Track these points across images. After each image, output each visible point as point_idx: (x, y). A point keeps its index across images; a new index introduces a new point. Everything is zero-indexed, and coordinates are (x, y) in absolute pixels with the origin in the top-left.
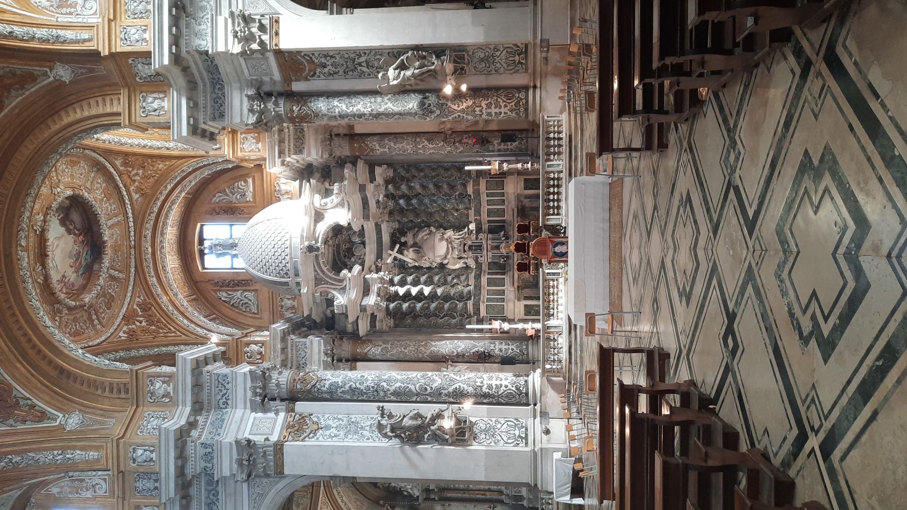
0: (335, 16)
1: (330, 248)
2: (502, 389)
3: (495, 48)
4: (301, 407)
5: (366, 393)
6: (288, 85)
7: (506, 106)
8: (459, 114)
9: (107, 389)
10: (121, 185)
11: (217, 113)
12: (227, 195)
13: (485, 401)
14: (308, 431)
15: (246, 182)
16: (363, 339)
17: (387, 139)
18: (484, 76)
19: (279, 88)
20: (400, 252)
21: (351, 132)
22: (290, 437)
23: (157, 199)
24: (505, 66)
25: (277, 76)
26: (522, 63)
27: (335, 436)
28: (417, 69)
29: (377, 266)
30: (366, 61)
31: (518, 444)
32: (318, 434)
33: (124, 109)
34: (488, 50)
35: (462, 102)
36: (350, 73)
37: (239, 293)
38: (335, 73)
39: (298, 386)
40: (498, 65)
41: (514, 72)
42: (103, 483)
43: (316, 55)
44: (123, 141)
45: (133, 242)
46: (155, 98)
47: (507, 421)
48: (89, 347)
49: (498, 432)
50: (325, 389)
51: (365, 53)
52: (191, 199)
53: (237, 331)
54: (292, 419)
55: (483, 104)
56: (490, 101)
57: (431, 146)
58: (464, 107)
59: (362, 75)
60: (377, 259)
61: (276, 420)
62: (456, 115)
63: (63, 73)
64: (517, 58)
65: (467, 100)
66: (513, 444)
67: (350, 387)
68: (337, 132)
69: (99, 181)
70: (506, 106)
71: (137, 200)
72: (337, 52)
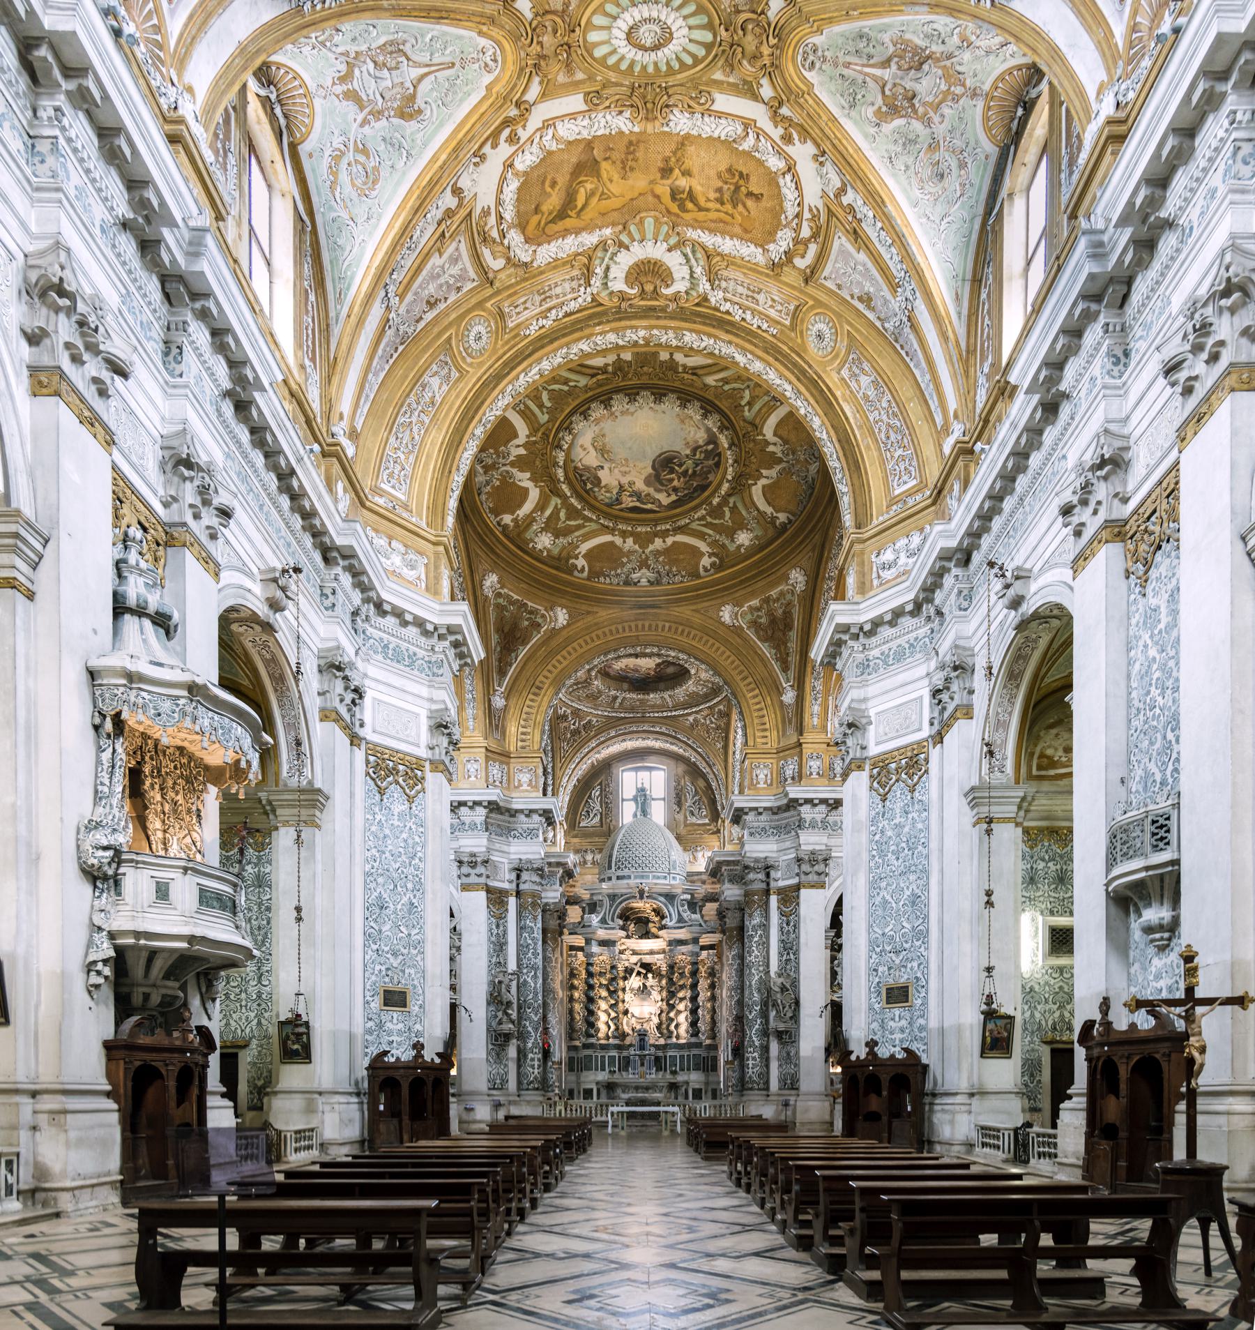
19: (773, 884)
25: (781, 884)
37: (598, 807)
59: (781, 955)
63: (789, 697)
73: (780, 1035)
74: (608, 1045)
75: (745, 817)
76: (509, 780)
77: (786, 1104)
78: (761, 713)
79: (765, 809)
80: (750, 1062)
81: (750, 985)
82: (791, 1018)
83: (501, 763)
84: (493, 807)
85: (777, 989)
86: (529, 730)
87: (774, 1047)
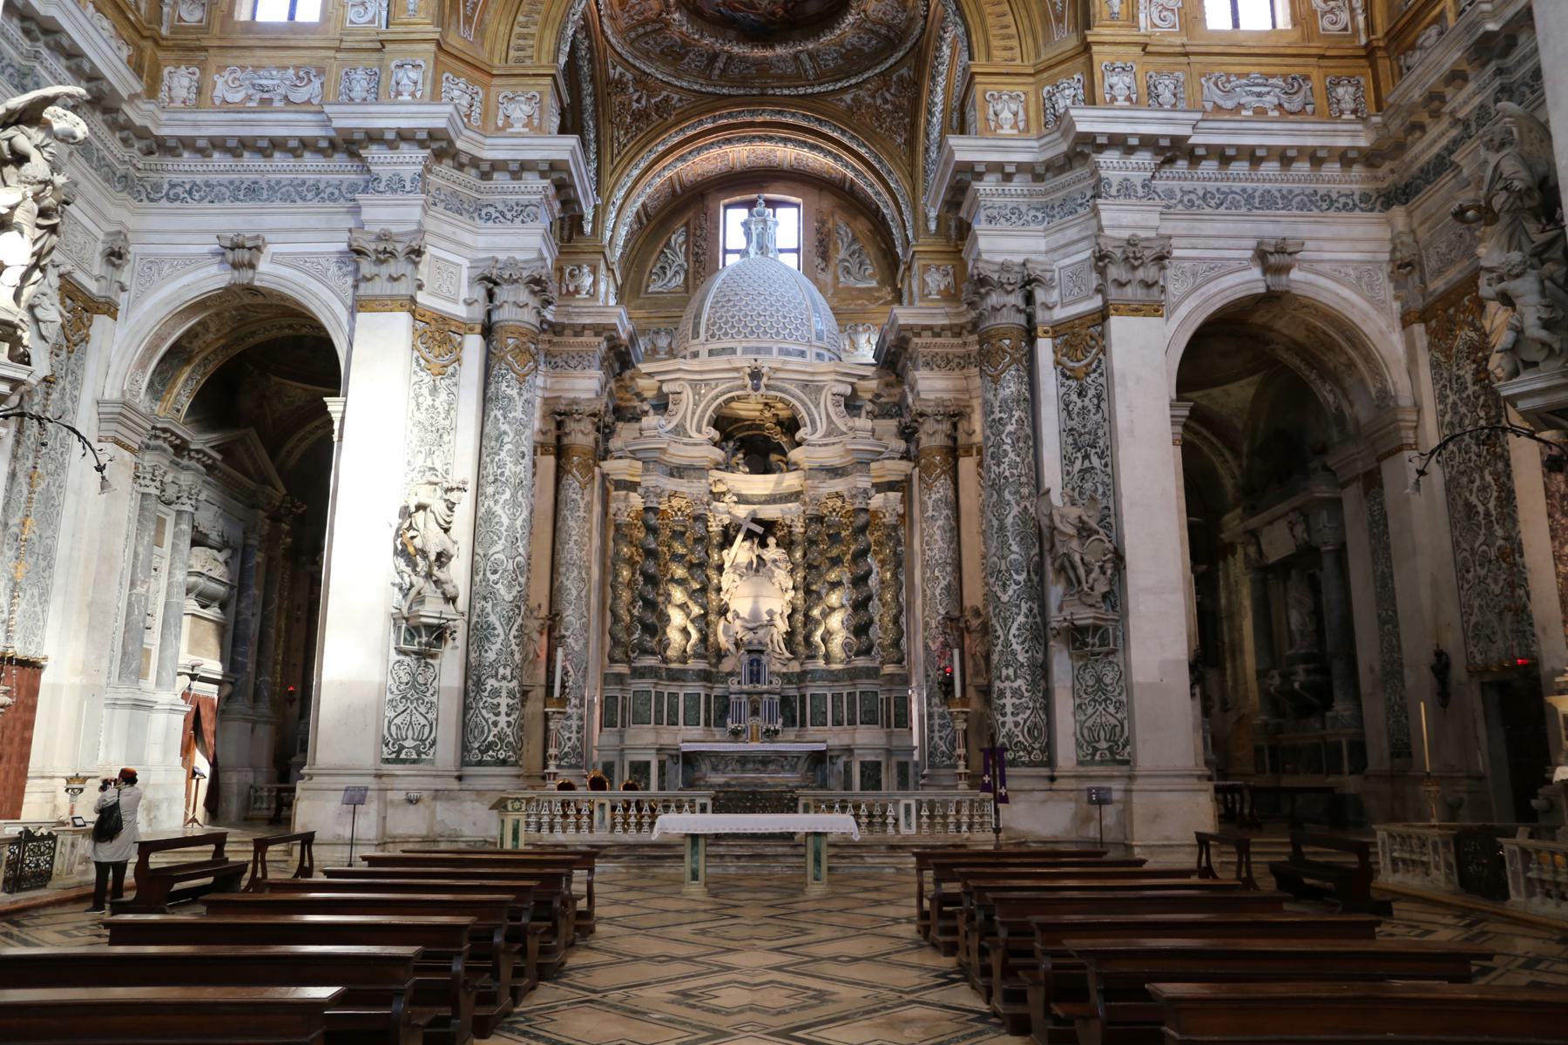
0: (1168, 412)
1: (758, 414)
2: (491, 715)
3: (1121, 702)
4: (473, 345)
5: (492, 461)
6: (1046, 332)
7: (1016, 724)
8: (1002, 638)
9: (525, 31)
10: (866, 76)
11: (994, 212)
12: (850, 245)
13: (470, 682)
14: (430, 356)
15: (872, 276)
16: (596, 469)
17: (949, 512)
18: (1069, 684)
19: (1041, 316)
20: (750, 535)
21: (961, 452)
22: (422, 324)
23: (843, 133)
24: (1089, 723)
25: (1059, 314)
26: (1093, 755)
27: (418, 405)
28: (1082, 559)
29: (724, 494)
30: (1093, 468)
31: (387, 745)
32: (424, 374)
33: (995, 65)
34: (1118, 691)
35: (1023, 643)
36: (1070, 440)
37: (681, 259)
38: (1069, 413)
39: (510, 341)
40: (1090, 711)
41: (1077, 740)
42: (362, 20)
43: (1102, 380)
44: (940, 79)
45: (771, 92)
46: (1015, 114)
47: (431, 725)
48: (600, 17)
49: (412, 707)
50: (503, 388)
51: (1106, 465)
52: (842, 188)
53: (618, 254)
54: (453, 329)
55: (1020, 682)
56: (1026, 694)
57: (938, 592)
58: (1015, 646)
59: (1067, 460)
60: (738, 495)
61: (455, 302)
62: (1000, 632)
64: (1104, 745)
65: (1027, 652)
66: (387, 735)
67: (505, 433)
68: (960, 425)
69: (874, 42)
70: (1016, 724)
71: (841, 100)
72: (1106, 416)
73: (1076, 636)
74: (684, 671)
75: (976, 185)
76: (485, 115)
77: (1101, 799)
78: (998, 9)
79: (1021, 167)
80: (1008, 701)
81: (1002, 528)
82: (1105, 596)
83: (471, 81)
84: (439, 146)
85: (1071, 531)
86: (533, 30)
87: (1062, 665)
